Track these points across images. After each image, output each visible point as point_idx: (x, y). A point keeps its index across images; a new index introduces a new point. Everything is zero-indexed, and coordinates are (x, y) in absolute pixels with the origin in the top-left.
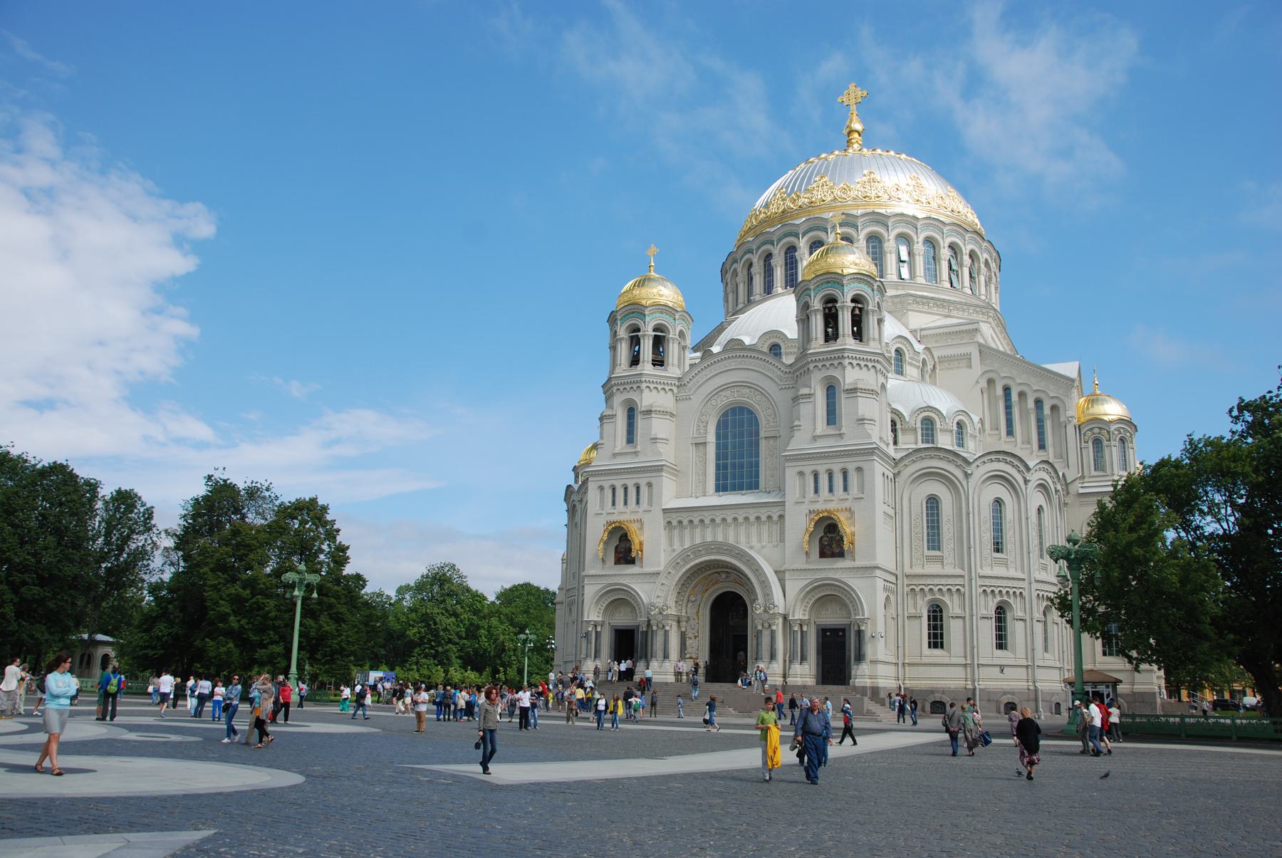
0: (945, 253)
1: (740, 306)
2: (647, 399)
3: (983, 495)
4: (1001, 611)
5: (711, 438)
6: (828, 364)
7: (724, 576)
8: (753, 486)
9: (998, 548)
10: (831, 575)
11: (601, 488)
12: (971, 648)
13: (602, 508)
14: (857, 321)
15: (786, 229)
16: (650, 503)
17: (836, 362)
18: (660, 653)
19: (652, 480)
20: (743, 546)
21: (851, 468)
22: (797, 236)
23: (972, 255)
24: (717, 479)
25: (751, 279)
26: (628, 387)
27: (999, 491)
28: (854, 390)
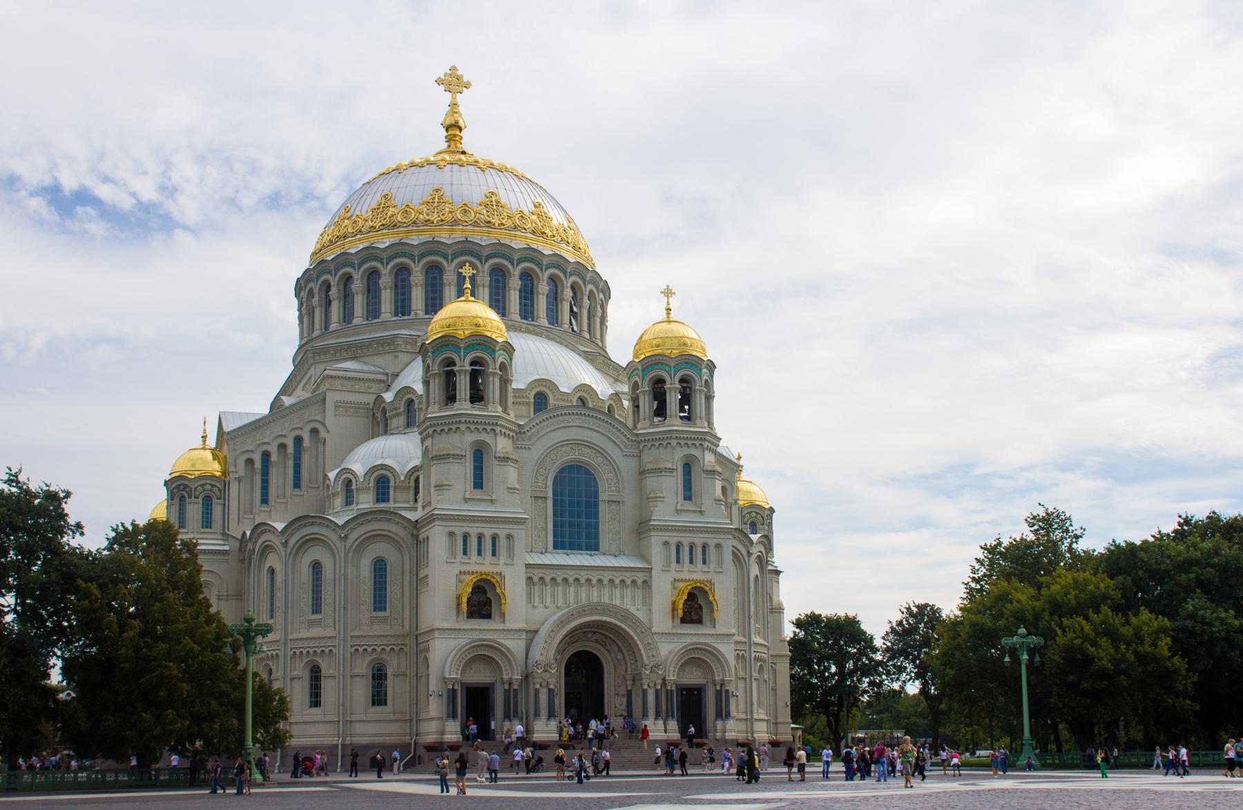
2: (502, 445)
5: (550, 494)
6: (690, 443)
7: (589, 635)
8: (592, 545)
9: (756, 622)
10: (702, 640)
11: (452, 534)
13: (453, 553)
16: (511, 555)
17: (697, 443)
19: (511, 532)
20: (633, 610)
21: (712, 543)
24: (555, 536)
26: (480, 428)
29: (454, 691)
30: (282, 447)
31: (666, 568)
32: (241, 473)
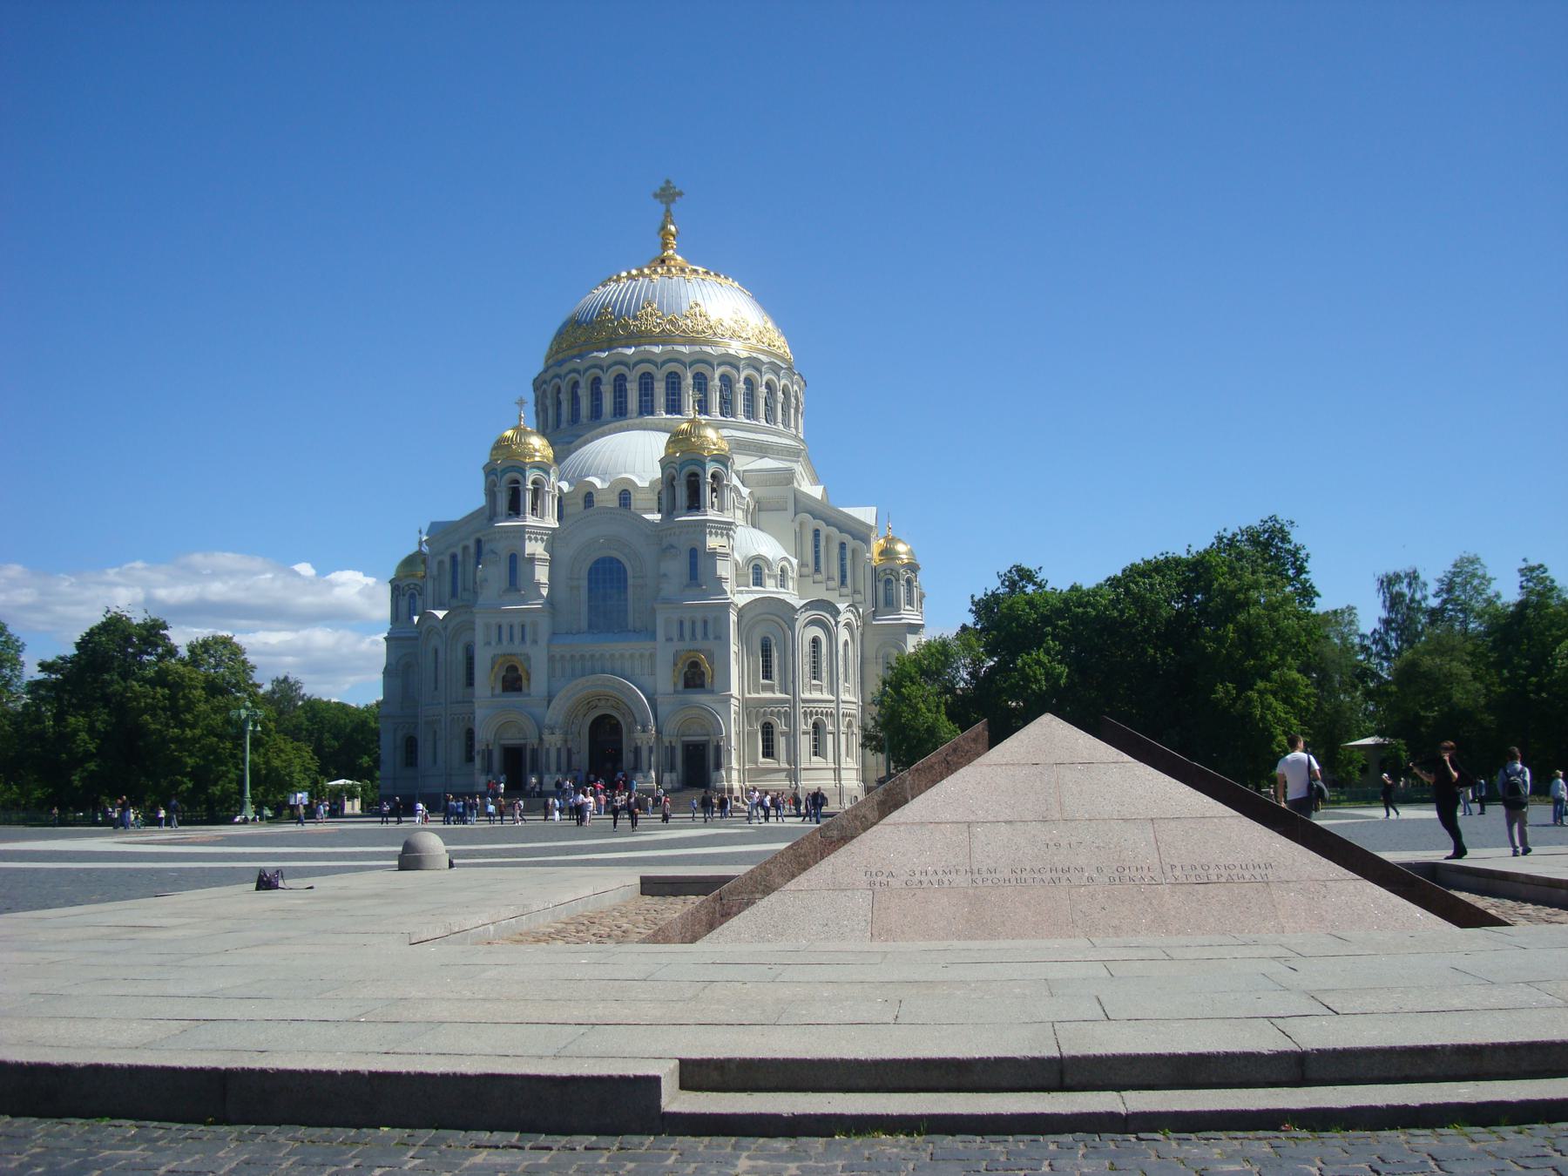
0: (763, 391)
1: (564, 425)
3: (806, 634)
4: (815, 725)
5: (585, 583)
9: (816, 674)
11: (487, 626)
12: (793, 758)
14: (713, 490)
15: (618, 358)
18: (553, 767)
22: (626, 365)
23: (785, 392)
25: (575, 399)
27: (817, 632)
28: (713, 555)
29: (490, 752)
30: (465, 548)
31: (669, 639)
32: (435, 572)
